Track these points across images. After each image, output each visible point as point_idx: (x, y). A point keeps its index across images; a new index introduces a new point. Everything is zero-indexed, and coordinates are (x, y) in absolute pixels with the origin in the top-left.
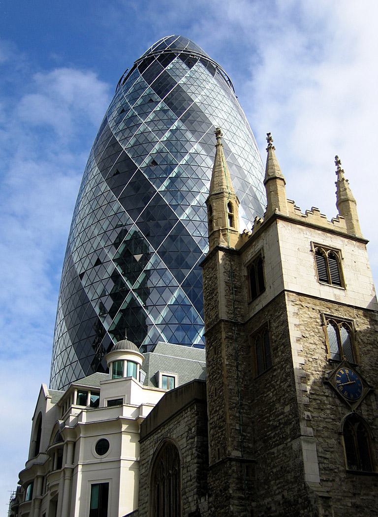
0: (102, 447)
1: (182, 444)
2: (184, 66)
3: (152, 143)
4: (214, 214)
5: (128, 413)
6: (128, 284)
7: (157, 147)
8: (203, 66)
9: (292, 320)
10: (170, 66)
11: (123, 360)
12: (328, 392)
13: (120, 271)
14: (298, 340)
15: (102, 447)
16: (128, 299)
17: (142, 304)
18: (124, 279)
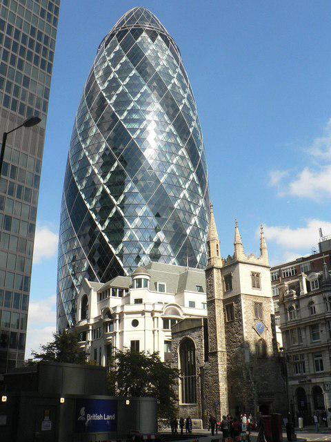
0: (135, 323)
1: (196, 341)
2: (149, 40)
3: (129, 102)
4: (211, 249)
5: (149, 308)
6: (114, 200)
7: (132, 104)
8: (162, 40)
9: (243, 306)
10: (140, 39)
11: (141, 279)
12: (253, 331)
13: (108, 191)
14: (245, 313)
15: (135, 323)
16: (114, 210)
17: (123, 214)
18: (112, 197)
